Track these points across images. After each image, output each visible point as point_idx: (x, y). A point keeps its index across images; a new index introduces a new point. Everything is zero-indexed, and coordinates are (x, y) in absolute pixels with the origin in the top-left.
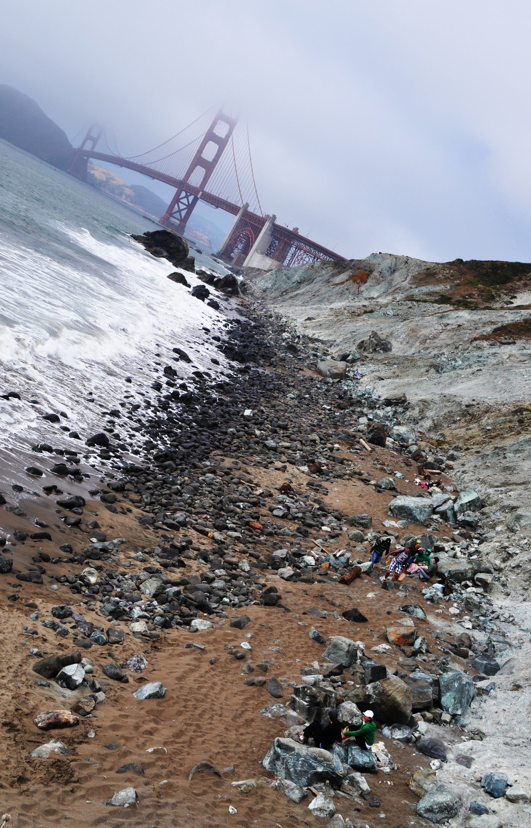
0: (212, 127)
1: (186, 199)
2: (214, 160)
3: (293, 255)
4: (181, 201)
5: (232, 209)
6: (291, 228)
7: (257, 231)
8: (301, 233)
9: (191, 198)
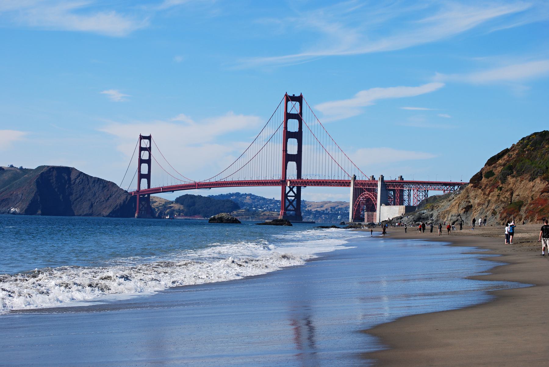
0: (286, 127)
1: (291, 192)
2: (298, 151)
3: (409, 195)
4: (288, 195)
5: (346, 184)
6: (398, 179)
7: (374, 191)
8: (405, 179)
9: (295, 190)
